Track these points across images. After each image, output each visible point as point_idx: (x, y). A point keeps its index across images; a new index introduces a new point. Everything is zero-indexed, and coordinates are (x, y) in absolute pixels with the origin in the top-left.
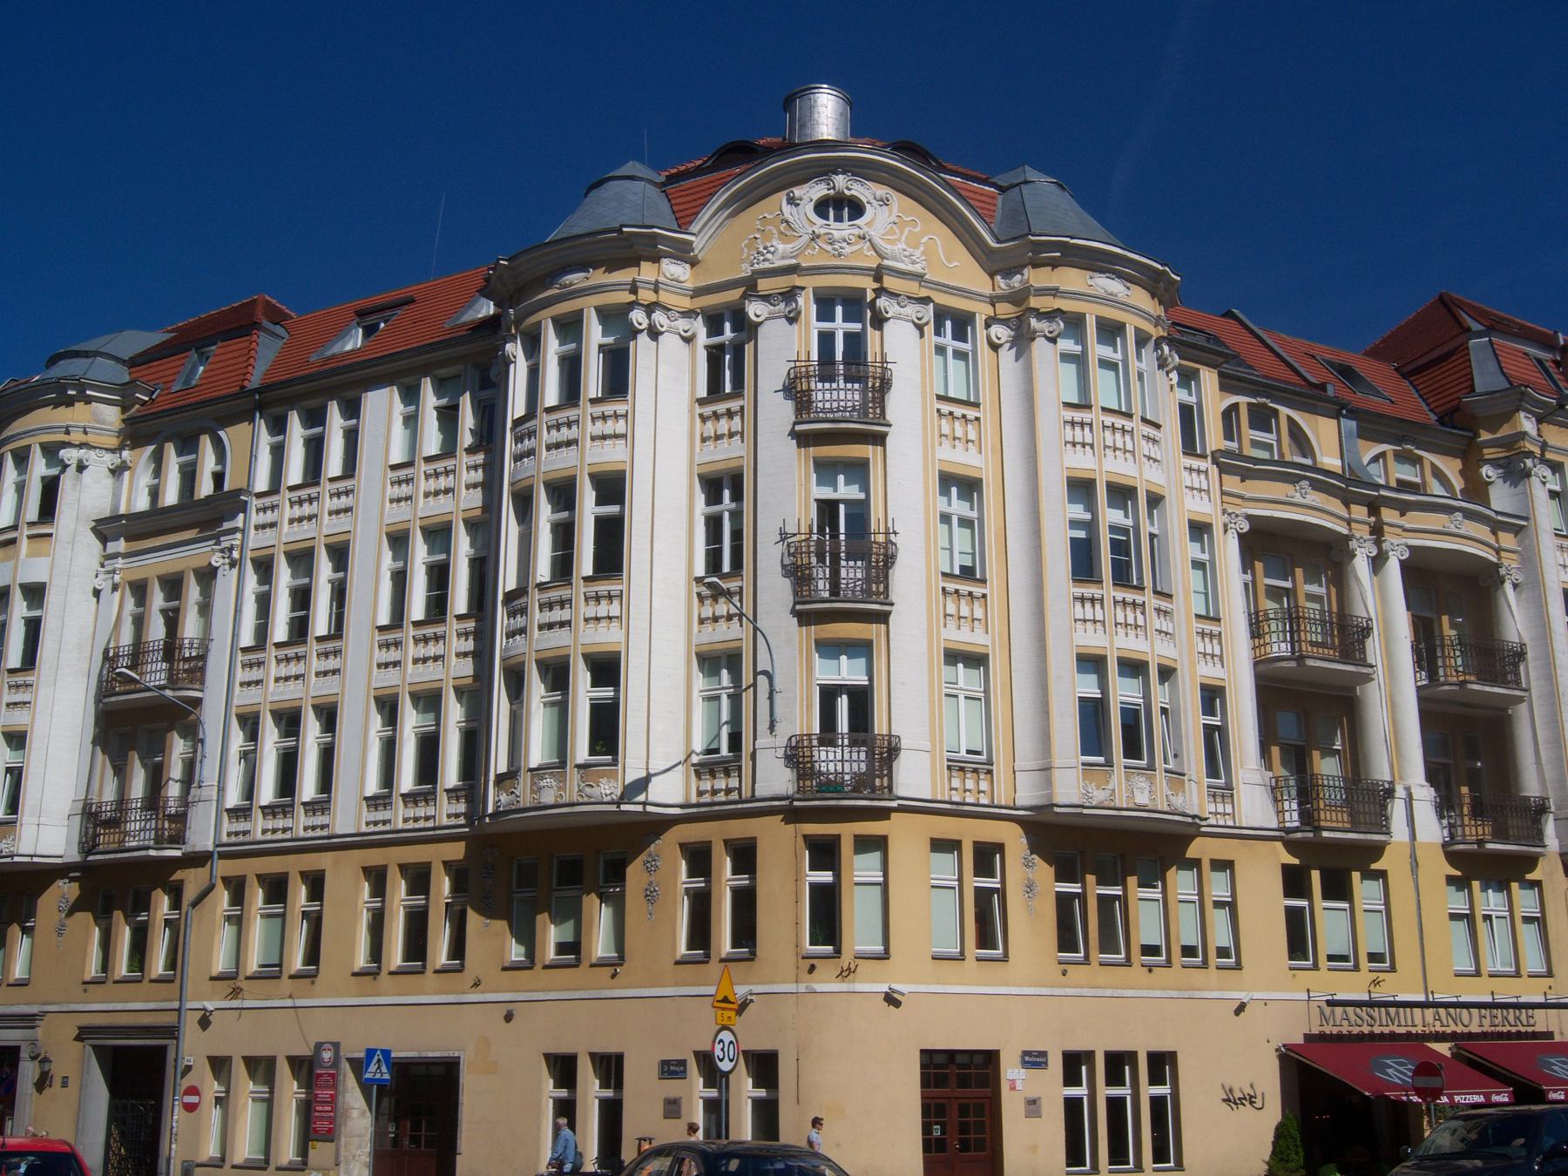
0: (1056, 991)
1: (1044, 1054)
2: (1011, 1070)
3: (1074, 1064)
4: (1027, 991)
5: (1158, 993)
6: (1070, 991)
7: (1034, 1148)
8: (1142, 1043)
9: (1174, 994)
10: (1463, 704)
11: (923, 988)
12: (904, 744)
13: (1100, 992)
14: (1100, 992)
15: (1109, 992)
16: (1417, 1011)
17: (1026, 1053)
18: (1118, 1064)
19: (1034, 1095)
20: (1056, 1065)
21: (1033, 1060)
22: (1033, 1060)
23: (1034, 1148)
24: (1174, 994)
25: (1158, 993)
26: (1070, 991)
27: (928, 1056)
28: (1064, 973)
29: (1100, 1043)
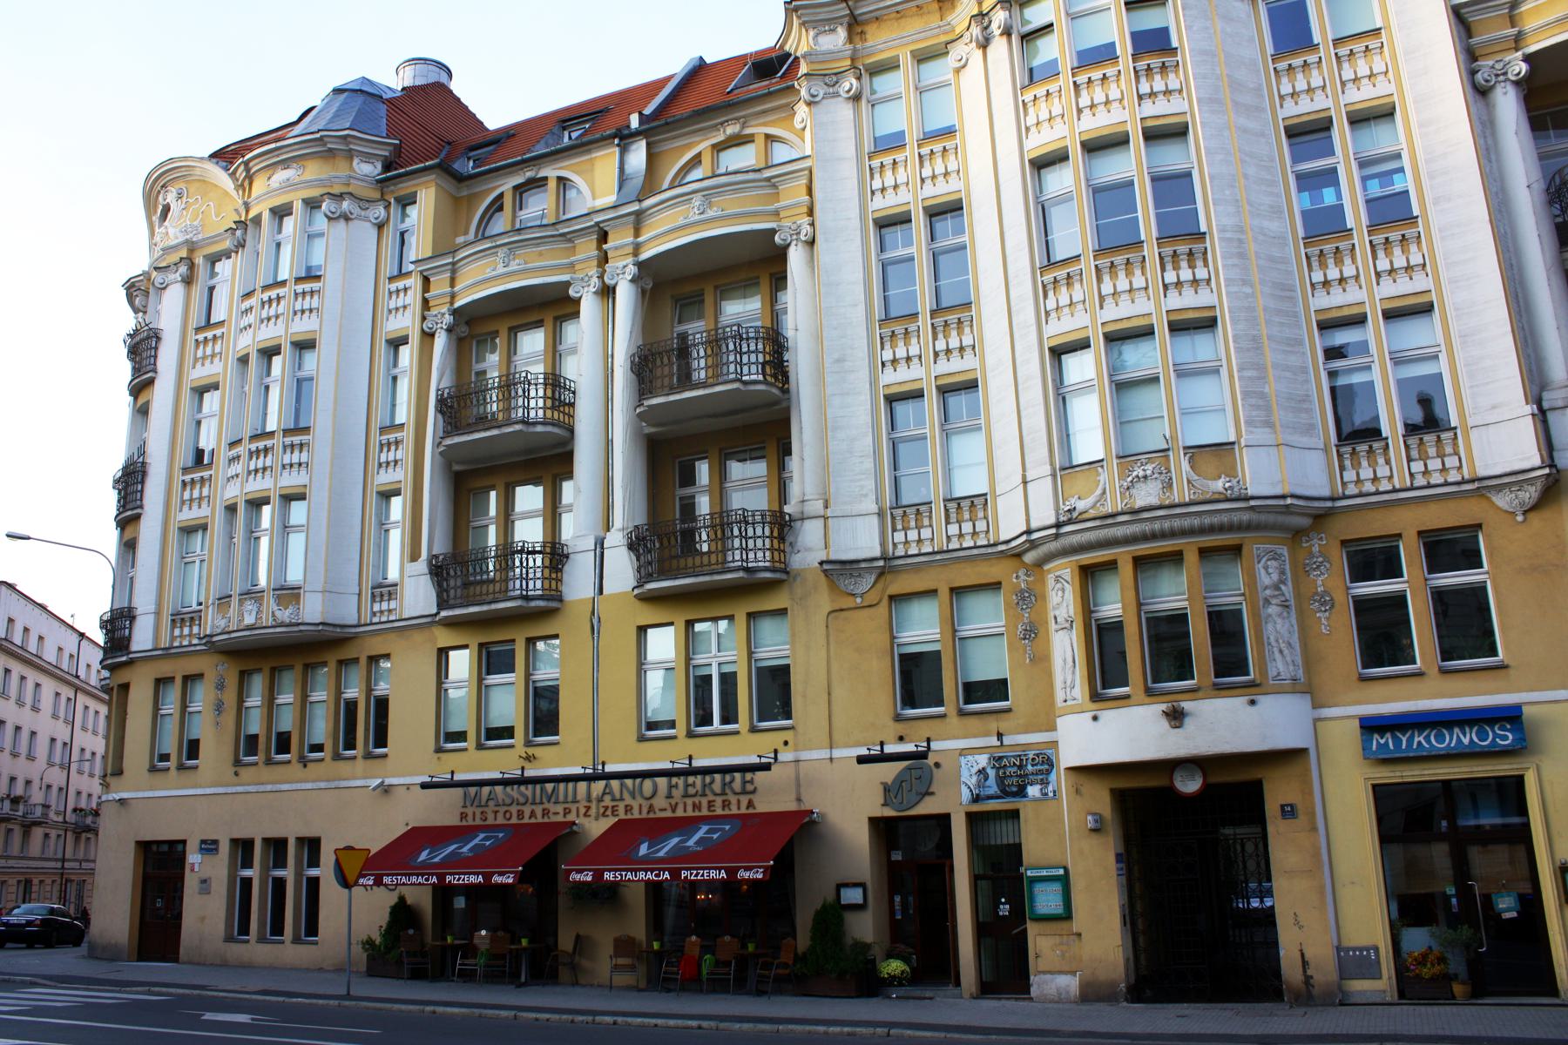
0: (230, 790)
1: (215, 842)
2: (193, 858)
3: (243, 848)
4: (208, 791)
5: (309, 786)
6: (240, 789)
7: (203, 919)
8: (291, 830)
9: (323, 785)
10: (715, 416)
11: (140, 795)
12: (138, 612)
13: (262, 788)
14: (262, 788)
15: (269, 787)
16: (582, 785)
17: (203, 842)
18: (277, 847)
19: (204, 876)
20: (225, 848)
21: (209, 847)
22: (209, 847)
23: (203, 919)
24: (323, 785)
25: (309, 786)
26: (240, 789)
27: (139, 844)
28: (236, 774)
29: (258, 830)
